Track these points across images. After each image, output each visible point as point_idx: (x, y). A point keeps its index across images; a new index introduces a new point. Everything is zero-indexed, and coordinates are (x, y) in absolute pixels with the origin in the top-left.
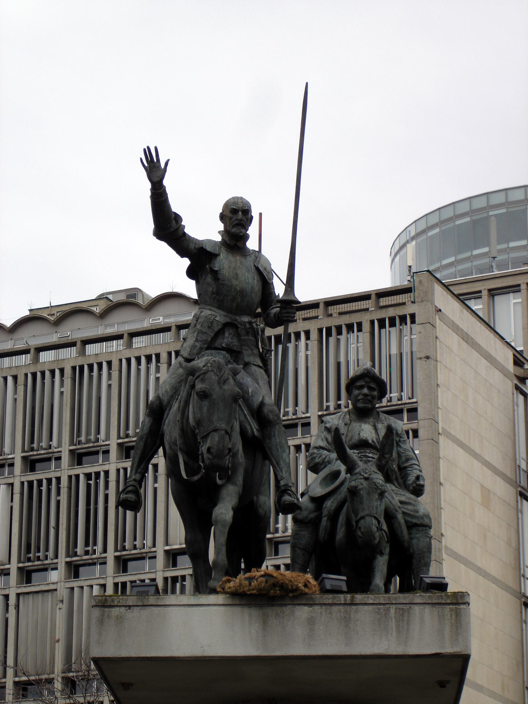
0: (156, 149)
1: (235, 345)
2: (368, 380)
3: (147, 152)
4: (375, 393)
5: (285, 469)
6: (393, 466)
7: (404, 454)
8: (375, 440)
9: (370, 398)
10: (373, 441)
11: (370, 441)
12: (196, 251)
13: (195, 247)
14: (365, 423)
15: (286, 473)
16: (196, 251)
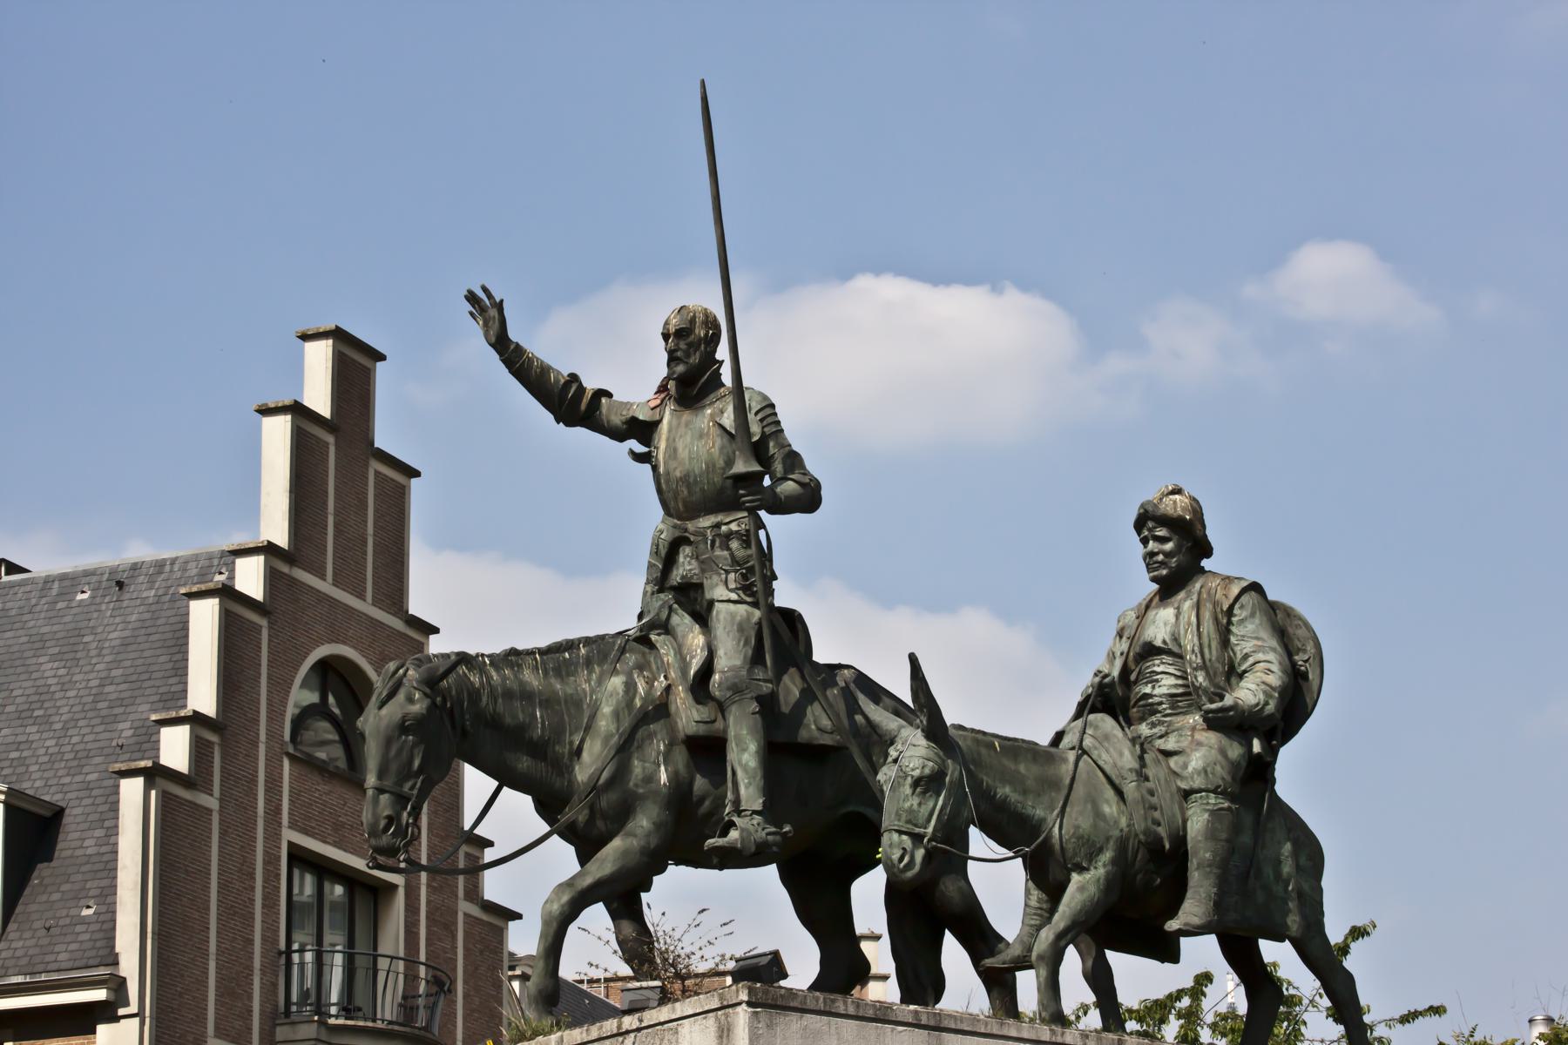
0: (485, 289)
1: (695, 574)
2: (1150, 524)
3: (471, 298)
4: (1169, 546)
5: (746, 781)
6: (1197, 681)
7: (1239, 648)
8: (1168, 641)
9: (1161, 557)
10: (1164, 642)
11: (1158, 643)
12: (625, 426)
13: (621, 421)
14: (1165, 606)
15: (747, 787)
16: (625, 426)
